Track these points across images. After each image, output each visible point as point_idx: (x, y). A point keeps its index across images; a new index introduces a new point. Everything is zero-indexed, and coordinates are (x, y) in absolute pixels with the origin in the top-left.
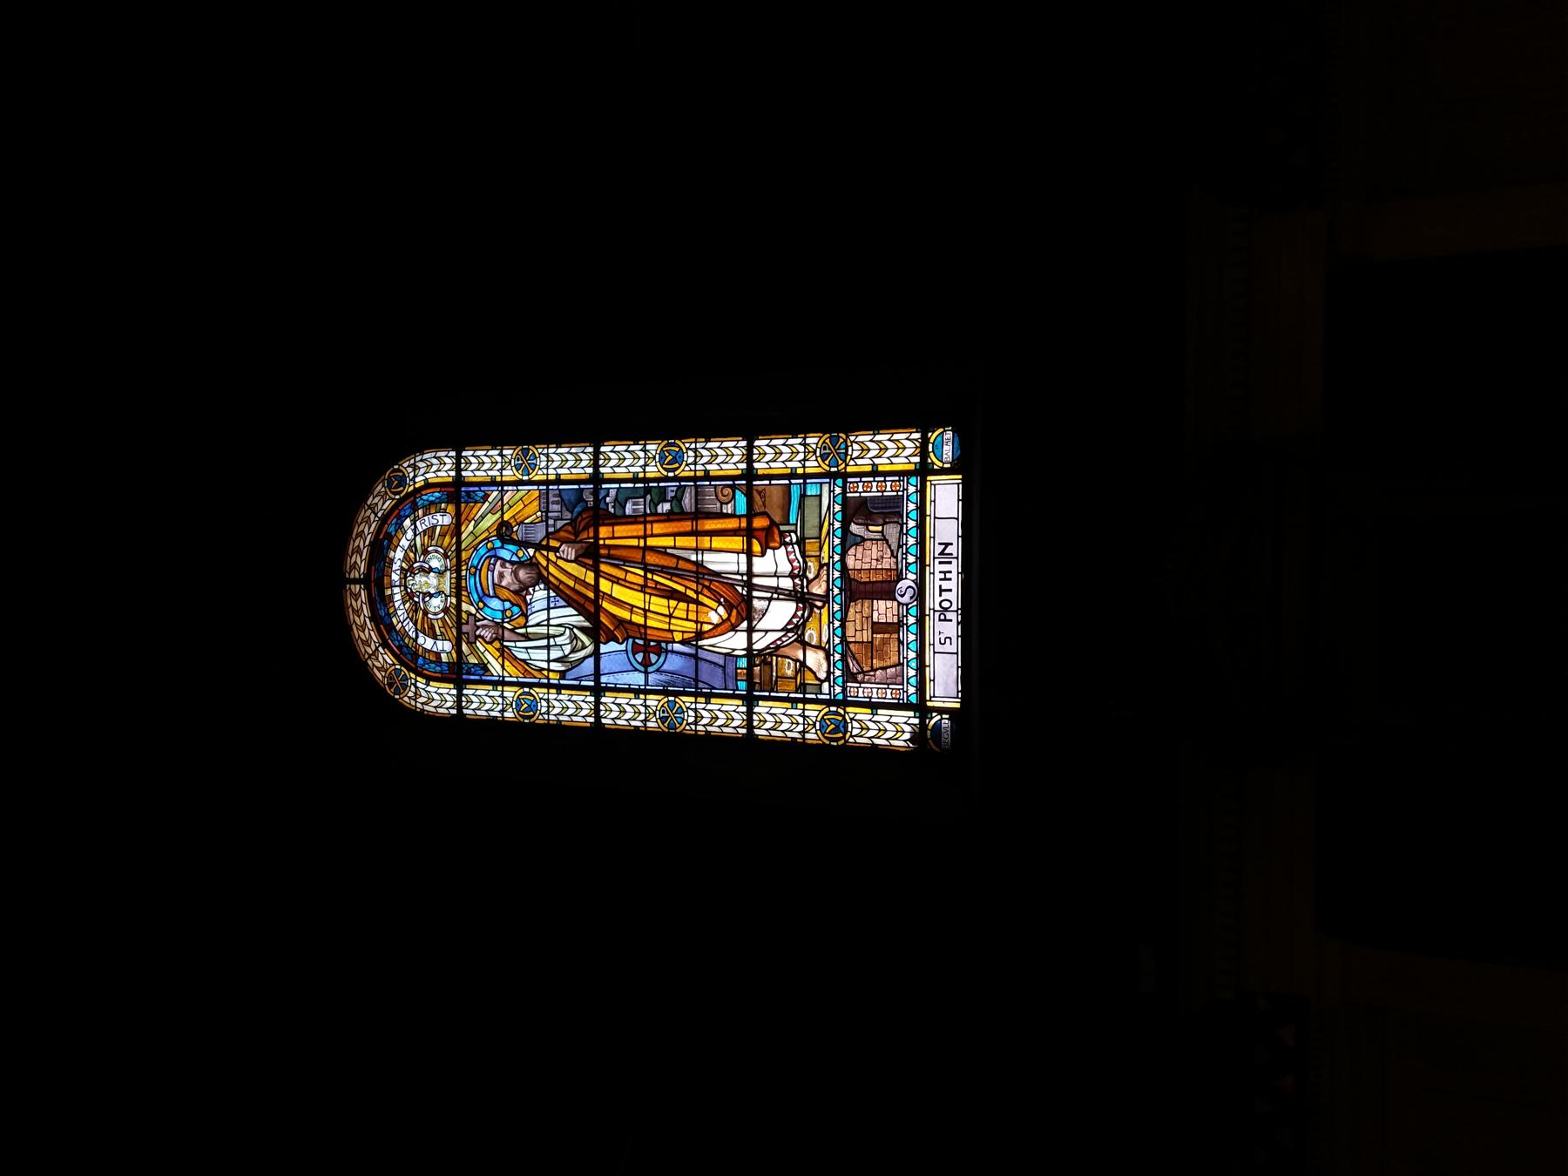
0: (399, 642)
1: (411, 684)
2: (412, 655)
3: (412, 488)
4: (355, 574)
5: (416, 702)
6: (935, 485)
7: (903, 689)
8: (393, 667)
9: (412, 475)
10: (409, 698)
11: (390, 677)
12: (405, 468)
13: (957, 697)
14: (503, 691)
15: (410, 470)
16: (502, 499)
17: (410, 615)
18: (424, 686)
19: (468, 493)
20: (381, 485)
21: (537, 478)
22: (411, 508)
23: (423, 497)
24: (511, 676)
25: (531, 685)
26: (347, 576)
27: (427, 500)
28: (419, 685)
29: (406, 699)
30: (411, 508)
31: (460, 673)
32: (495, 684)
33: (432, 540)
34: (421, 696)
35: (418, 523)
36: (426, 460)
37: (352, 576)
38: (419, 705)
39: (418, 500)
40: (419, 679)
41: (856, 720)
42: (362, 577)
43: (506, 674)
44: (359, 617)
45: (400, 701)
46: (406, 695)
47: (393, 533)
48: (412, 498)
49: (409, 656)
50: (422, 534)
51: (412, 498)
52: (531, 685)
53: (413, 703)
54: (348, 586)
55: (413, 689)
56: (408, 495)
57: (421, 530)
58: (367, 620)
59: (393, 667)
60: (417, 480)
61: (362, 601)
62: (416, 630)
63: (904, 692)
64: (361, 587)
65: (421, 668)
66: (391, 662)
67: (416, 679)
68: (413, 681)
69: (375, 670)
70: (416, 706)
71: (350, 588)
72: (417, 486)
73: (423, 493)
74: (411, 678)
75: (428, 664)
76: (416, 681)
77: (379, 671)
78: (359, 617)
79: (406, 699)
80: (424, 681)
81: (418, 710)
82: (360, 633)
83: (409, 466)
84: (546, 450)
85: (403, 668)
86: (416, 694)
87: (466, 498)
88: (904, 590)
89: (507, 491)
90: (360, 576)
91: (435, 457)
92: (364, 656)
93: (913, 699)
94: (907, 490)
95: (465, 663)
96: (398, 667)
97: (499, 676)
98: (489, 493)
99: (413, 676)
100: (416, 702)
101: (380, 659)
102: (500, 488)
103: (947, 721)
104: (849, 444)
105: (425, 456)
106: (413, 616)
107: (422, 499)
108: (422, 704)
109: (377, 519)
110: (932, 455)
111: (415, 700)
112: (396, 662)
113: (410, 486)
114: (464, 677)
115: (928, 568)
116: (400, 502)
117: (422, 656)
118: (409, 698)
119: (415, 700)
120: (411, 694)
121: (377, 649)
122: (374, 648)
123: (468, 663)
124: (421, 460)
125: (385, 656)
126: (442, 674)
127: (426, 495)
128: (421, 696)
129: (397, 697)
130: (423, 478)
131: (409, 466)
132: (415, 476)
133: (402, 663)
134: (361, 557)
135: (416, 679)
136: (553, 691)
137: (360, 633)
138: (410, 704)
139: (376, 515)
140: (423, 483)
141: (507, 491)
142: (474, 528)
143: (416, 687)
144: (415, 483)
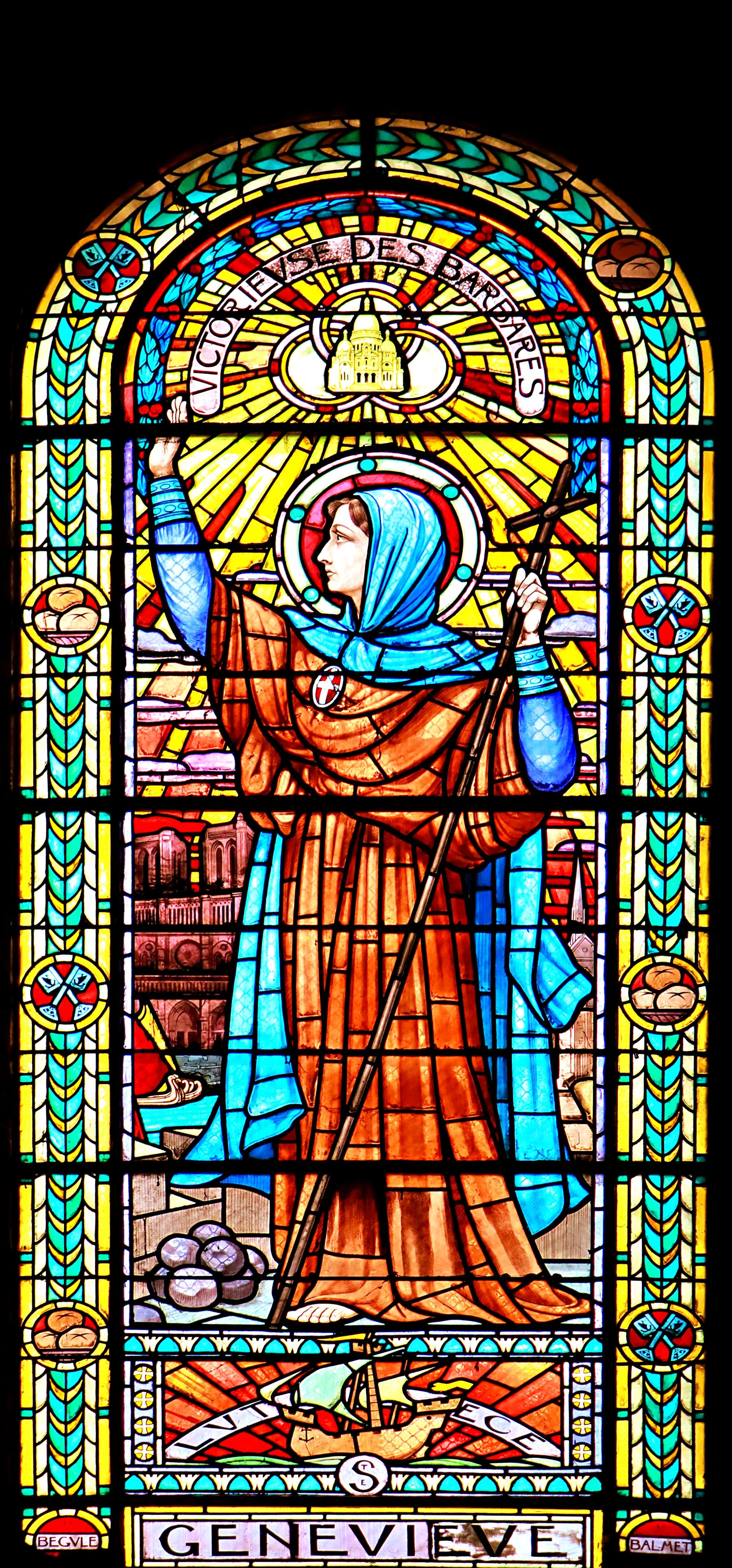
0: (213, 263)
1: (105, 303)
3: (610, 306)
6: (584, 1523)
7: (155, 1465)
8: (144, 254)
9: (646, 307)
10: (68, 300)
12: (663, 287)
13: (143, 1560)
15: (658, 300)
18: (100, 336)
21: (627, 647)
23: (587, 334)
27: (578, 346)
28: (103, 321)
29: (64, 291)
30: (560, 301)
34: (75, 329)
38: (51, 324)
39: (580, 320)
41: (83, 1378)
42: (379, 164)
47: (494, 245)
50: (493, 336)
53: (57, 309)
54: (356, 123)
55: (91, 308)
58: (266, 181)
59: (144, 254)
60: (632, 321)
63: (149, 1467)
66: (157, 247)
68: (111, 308)
70: (47, 316)
72: (617, 321)
73: (598, 336)
74: (119, 301)
75: (158, 347)
76: (112, 316)
81: (36, 324)
83: (668, 297)
85: (143, 278)
86: (80, 315)
88: (368, 1470)
91: (687, 368)
93: (132, 1484)
99: (125, 306)
102: (604, 542)
103: (95, 1543)
104: (676, 1367)
107: (582, 331)
108: (55, 334)
110: (646, 1517)
111: (64, 314)
113: (616, 300)
115: (411, 1510)
116: (578, 276)
120: (78, 303)
122: (193, 198)
126: (135, 384)
127: (593, 341)
128: (75, 329)
129: (68, 266)
130: (636, 336)
131: (668, 297)
132: (640, 314)
138: (53, 302)
140: (622, 335)
143: (96, 315)
144: (624, 315)
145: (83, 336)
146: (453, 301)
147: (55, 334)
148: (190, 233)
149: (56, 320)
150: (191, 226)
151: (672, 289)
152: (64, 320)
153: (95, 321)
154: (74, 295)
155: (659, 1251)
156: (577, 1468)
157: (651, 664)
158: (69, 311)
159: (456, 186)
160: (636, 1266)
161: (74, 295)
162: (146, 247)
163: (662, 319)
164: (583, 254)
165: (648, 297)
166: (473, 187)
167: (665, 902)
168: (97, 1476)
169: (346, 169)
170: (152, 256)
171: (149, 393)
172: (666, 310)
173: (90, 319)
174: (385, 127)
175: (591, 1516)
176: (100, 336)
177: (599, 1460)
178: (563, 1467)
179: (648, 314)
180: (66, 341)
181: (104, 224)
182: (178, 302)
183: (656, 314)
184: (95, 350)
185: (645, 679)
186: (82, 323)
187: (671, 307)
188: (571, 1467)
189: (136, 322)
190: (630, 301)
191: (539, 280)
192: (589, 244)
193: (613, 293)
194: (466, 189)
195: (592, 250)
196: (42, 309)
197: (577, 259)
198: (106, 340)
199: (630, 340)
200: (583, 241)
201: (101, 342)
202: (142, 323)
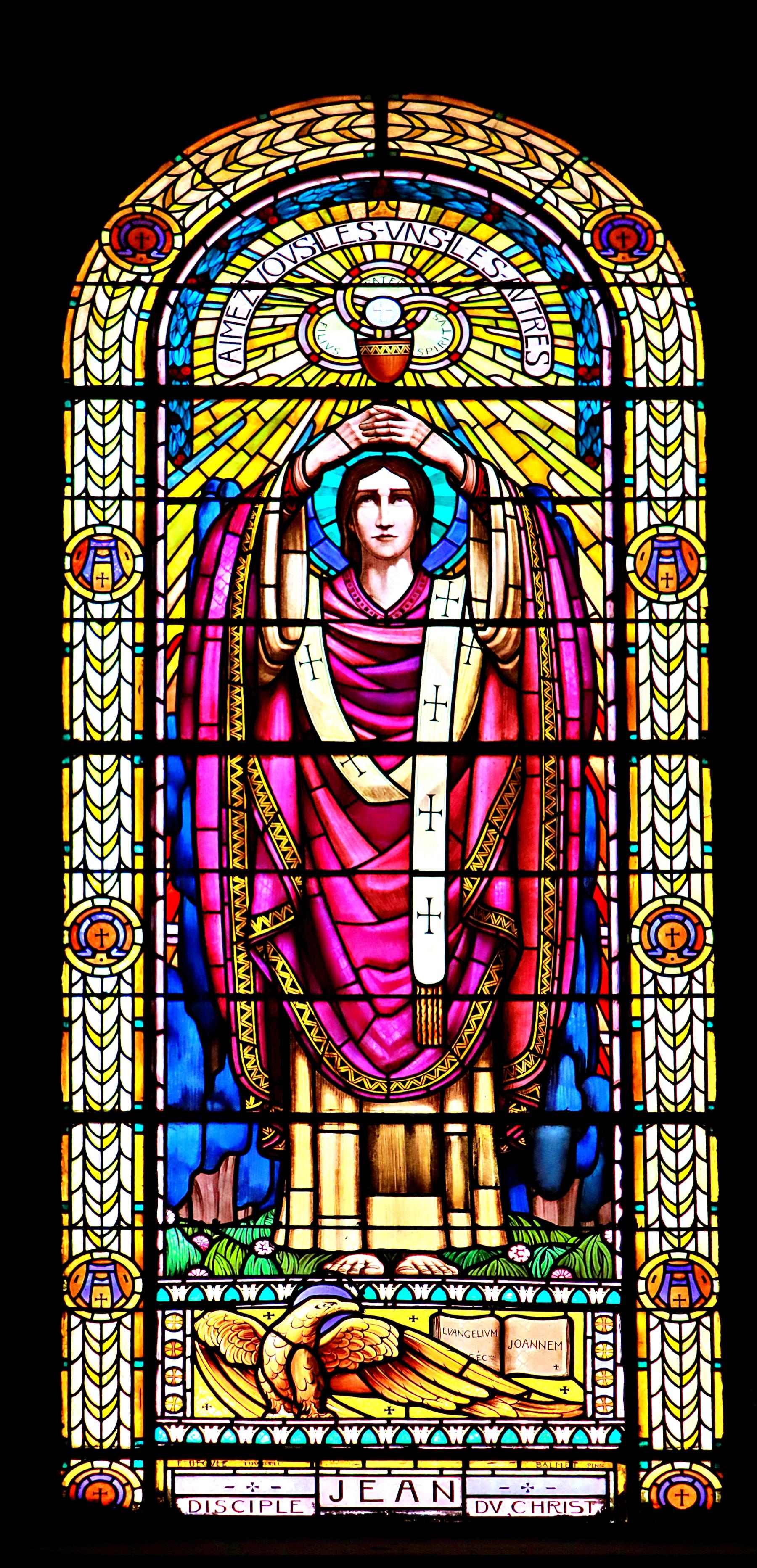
1: (140, 275)
2: (206, 274)
3: (609, 279)
4: (396, 122)
5: (96, 284)
8: (176, 229)
10: (104, 270)
11: (150, 221)
12: (657, 261)
15: (652, 274)
16: (583, 500)
17: (303, 269)
19: (598, 420)
20: (616, 195)
22: (564, 273)
24: (167, 522)
26: (394, 105)
28: (139, 291)
29: (101, 261)
31: (170, 393)
33: (485, 327)
34: (111, 298)
36: (675, 314)
37: (394, 118)
44: (296, 138)
45: (96, 246)
46: (109, 261)
48: (586, 278)
49: (202, 269)
50: (501, 303)
51: (586, 278)
53: (94, 278)
55: (127, 277)
58: (288, 161)
59: (176, 229)
60: (628, 291)
61: (334, 145)
62: (268, 287)
64: (370, 141)
66: (188, 222)
67: (151, 284)
68: (146, 279)
69: (165, 181)
71: (365, 112)
72: (614, 291)
74: (153, 274)
76: (146, 287)
77: (165, 190)
78: (296, 138)
79: (101, 261)
80: (148, 305)
82: (256, 141)
83: (661, 270)
84: (694, 616)
85: (175, 253)
86: (116, 285)
87: (587, 415)
89: (602, 515)
90: (394, 140)
92: (198, 151)
94: (597, 1426)
95: (192, 407)
96: (178, 242)
97: (167, 491)
98: (599, 470)
99: (159, 278)
101: (194, 196)
105: (683, 313)
106: (303, 276)
108: (92, 302)
109: (537, 188)
112: (190, 236)
113: (613, 272)
117: (204, 301)
118: (104, 270)
119: (100, 283)
120: (113, 273)
123: (193, 416)
124: (673, 303)
125: (201, 208)
128: (111, 298)
129: (105, 237)
130: (631, 306)
131: (661, 270)
132: (634, 285)
133: (187, 253)
134: (440, 143)
135: (151, 284)
137: (256, 141)
138: (89, 271)
139: (549, 185)
141: (602, 515)
142: (516, 433)
144: (620, 286)
145: (118, 305)
146: (462, 274)
149: (93, 288)
150: (219, 204)
151: (665, 262)
152: (100, 288)
153: (132, 290)
154: (110, 266)
155: (674, 1168)
156: (598, 1420)
157: (652, 611)
158: (106, 280)
159: (463, 166)
160: (653, 1216)
161: (110, 266)
162: (177, 221)
163: (656, 290)
164: (582, 228)
165: (643, 270)
166: (479, 167)
167: (674, 1035)
168: (132, 1193)
169: (363, 151)
170: (184, 230)
172: (660, 281)
173: (128, 288)
174: (398, 112)
175: (615, 1470)
176: (135, 307)
177: (621, 1413)
178: (583, 1417)
179: (642, 285)
180: (103, 309)
181: (137, 199)
183: (650, 285)
184: (130, 318)
185: (647, 625)
186: (118, 292)
187: (664, 278)
188: (593, 1418)
189: (168, 295)
190: (627, 274)
191: (544, 255)
192: (588, 220)
193: (611, 266)
194: (472, 168)
195: (589, 227)
196: (80, 278)
197: (577, 233)
198: (141, 310)
199: (626, 309)
200: (582, 216)
201: (136, 311)
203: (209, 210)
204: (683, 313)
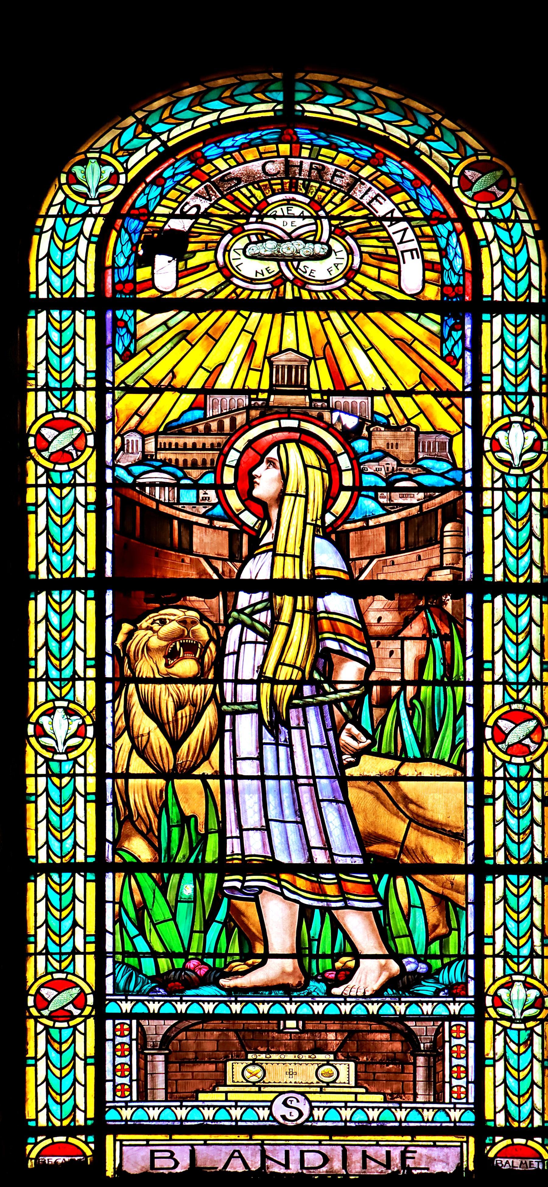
10: (63, 203)
14: (85, 389)
25: (99, 447)
28: (89, 221)
29: (60, 197)
32: (100, 373)
35: (404, 225)
40: (100, 221)
43: (118, 394)
52: (99, 447)
53: (54, 211)
56: (458, 205)
57: (391, 230)
59: (120, 169)
65: (122, 226)
73: (463, 237)
74: (101, 205)
76: (96, 216)
80: (97, 231)
96: (122, 179)
99: (106, 210)
100: (56, 217)
105: (531, 242)
112: (132, 175)
114: (109, 315)
120: (70, 205)
121: (156, 136)
125: (142, 153)
127: (458, 241)
130: (491, 236)
136: (92, 495)
138: (51, 205)
143: (84, 216)
147: (53, 228)
148: (155, 154)
170: (127, 171)
171: (124, 274)
182: (146, 206)
202: (119, 222)
203: (147, 154)
204: (531, 242)
